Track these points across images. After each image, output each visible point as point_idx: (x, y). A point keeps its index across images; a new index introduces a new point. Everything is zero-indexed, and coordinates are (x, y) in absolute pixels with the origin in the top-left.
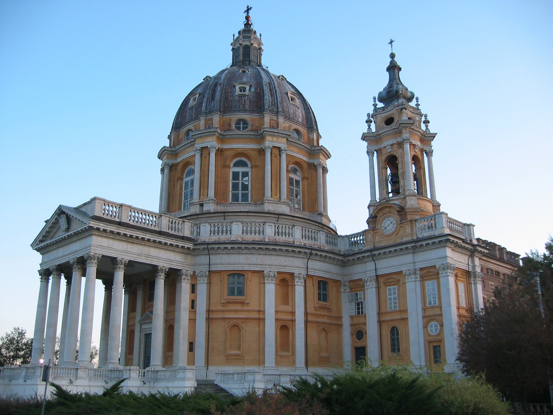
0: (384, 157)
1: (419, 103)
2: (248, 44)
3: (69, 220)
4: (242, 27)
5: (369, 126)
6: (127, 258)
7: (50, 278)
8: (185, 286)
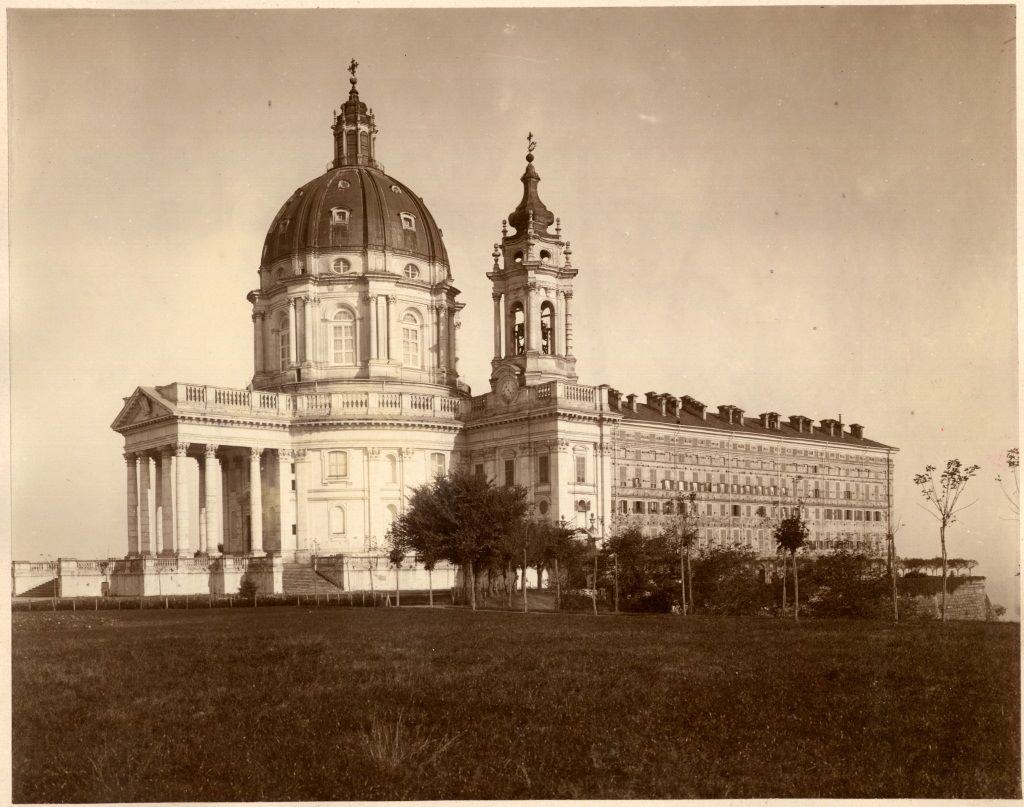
0: (510, 303)
1: (560, 226)
2: (354, 128)
3: (150, 402)
4: (345, 98)
5: (496, 261)
6: (217, 443)
7: (138, 462)
8: (284, 467)
